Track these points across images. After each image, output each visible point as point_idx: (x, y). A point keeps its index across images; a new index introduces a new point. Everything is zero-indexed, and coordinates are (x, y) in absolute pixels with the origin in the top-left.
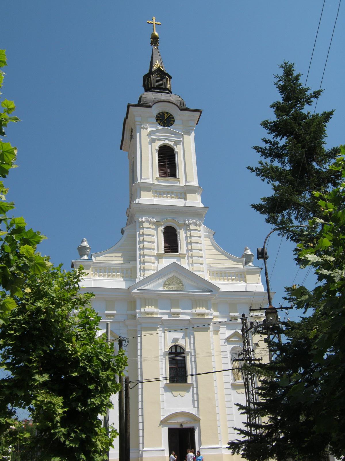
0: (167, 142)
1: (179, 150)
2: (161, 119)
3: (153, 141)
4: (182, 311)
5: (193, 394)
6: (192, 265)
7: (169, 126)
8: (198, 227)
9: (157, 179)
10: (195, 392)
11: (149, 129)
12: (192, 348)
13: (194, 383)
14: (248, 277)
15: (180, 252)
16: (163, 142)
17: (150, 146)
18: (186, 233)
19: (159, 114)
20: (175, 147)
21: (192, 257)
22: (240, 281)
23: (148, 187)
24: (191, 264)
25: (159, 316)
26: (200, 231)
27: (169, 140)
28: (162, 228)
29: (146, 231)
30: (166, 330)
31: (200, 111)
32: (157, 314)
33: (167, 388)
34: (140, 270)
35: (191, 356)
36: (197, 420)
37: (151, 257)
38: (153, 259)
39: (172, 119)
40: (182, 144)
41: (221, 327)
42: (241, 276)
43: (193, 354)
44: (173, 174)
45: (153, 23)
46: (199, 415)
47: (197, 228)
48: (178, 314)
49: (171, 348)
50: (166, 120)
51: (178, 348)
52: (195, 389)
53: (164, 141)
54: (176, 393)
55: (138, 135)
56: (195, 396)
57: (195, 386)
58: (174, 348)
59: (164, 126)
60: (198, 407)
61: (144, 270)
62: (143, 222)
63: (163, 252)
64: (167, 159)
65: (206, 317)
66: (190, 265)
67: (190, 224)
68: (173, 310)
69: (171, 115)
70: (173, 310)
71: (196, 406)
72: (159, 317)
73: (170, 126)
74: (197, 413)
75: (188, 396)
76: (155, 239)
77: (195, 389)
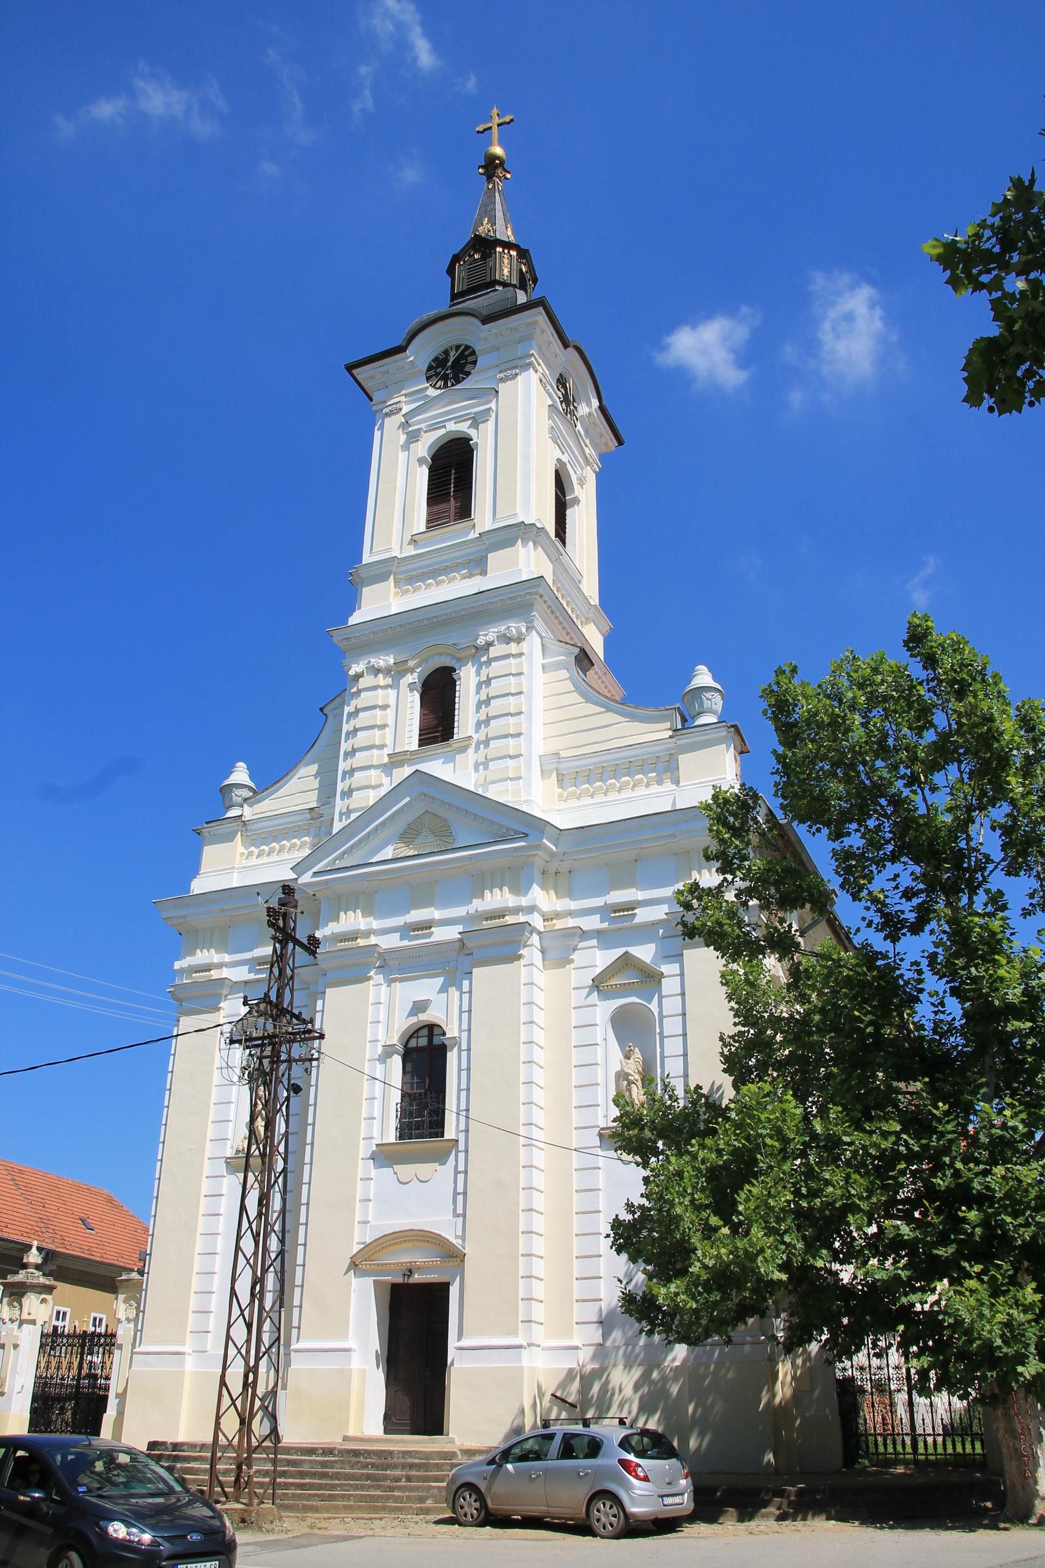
0: (452, 427)
1: (483, 440)
2: (439, 370)
3: (413, 437)
4: (437, 914)
5: (457, 1172)
6: (486, 768)
7: (458, 381)
8: (513, 645)
9: (413, 541)
10: (461, 1168)
11: (406, 409)
12: (465, 1026)
13: (462, 1138)
14: (684, 759)
15: (455, 737)
16: (443, 431)
17: (402, 456)
18: (478, 674)
19: (436, 359)
20: (473, 433)
21: (486, 742)
22: (660, 782)
23: (382, 571)
24: (482, 763)
25: (373, 940)
26: (520, 655)
27: (459, 420)
28: (412, 678)
29: (365, 699)
30: (394, 980)
31: (541, 303)
32: (367, 934)
33: (383, 1156)
34: (341, 814)
35: (460, 1051)
36: (454, 1256)
37: (373, 772)
38: (374, 776)
39: (470, 359)
40: (493, 419)
41: (581, 945)
42: (664, 766)
43: (464, 1046)
44: (464, 512)
45: (490, 128)
46: (464, 1240)
47: (513, 648)
48: (426, 926)
49: (415, 1033)
50: (453, 367)
51: (436, 1031)
52: (462, 1156)
53: (444, 426)
54: (405, 1170)
55: (377, 434)
56: (461, 1177)
57: (461, 1146)
58: (425, 1032)
59: (446, 386)
60: (464, 1215)
61: (349, 812)
62: (358, 676)
63: (414, 746)
64: (452, 474)
65: (510, 919)
66: (481, 767)
67: (490, 644)
68: (417, 915)
69: (467, 347)
70: (417, 915)
71: (460, 1210)
72: (373, 943)
73: (464, 379)
74: (459, 1233)
75: (441, 1175)
76: (390, 715)
77: (462, 1156)
